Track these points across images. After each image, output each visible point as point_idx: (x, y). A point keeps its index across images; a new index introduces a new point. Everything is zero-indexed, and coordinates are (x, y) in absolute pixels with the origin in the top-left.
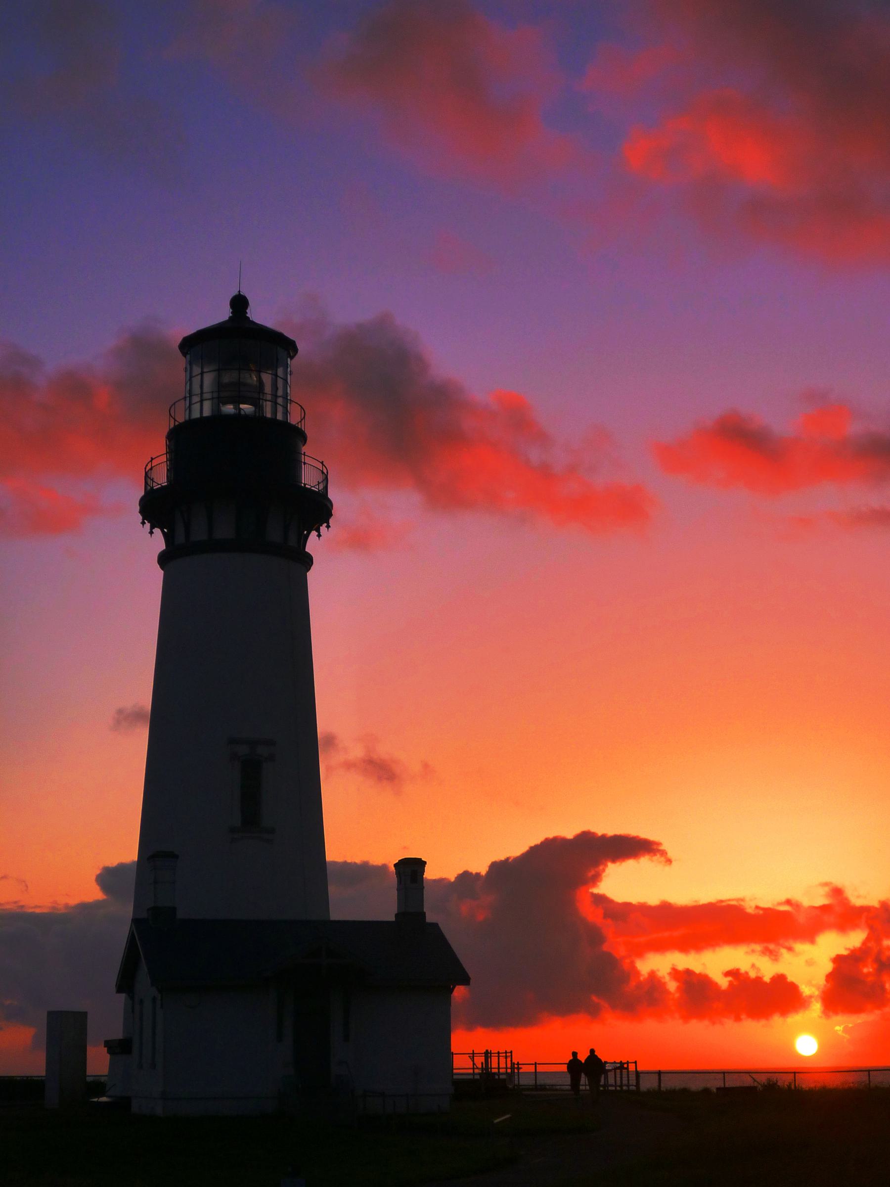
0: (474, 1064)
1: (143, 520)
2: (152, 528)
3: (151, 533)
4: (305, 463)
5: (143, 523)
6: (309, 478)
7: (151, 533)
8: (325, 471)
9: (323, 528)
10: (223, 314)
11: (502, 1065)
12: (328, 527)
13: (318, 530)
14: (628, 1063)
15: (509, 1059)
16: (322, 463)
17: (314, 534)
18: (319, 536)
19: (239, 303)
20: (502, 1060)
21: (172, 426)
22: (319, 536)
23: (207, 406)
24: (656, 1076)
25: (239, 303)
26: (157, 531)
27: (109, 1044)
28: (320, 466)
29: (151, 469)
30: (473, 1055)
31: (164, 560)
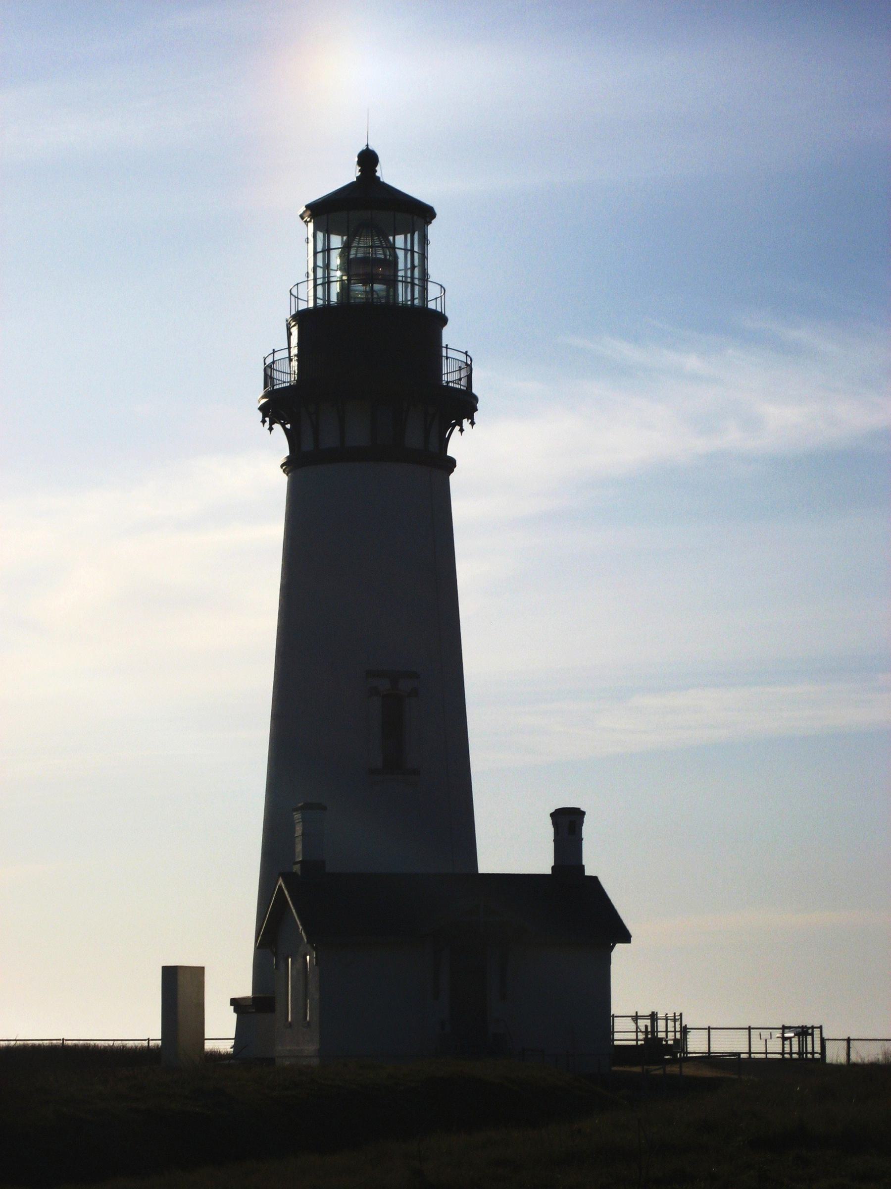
0: (637, 1027)
1: (264, 417)
2: (271, 424)
3: (271, 429)
4: (447, 358)
5: (264, 422)
6: (450, 375)
7: (271, 429)
8: (469, 362)
9: (466, 423)
10: (350, 174)
11: (671, 1028)
12: (473, 423)
13: (461, 425)
14: (813, 1028)
15: (678, 1023)
16: (466, 353)
17: (457, 428)
18: (462, 430)
19: (368, 159)
20: (671, 1024)
21: (293, 312)
22: (462, 430)
23: (336, 288)
24: (845, 1043)
25: (368, 159)
26: (277, 427)
27: (236, 1003)
28: (463, 357)
29: (273, 362)
30: (636, 1018)
31: (289, 466)
